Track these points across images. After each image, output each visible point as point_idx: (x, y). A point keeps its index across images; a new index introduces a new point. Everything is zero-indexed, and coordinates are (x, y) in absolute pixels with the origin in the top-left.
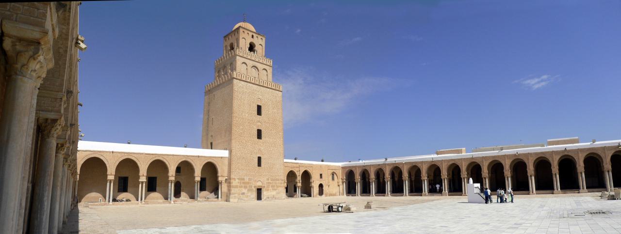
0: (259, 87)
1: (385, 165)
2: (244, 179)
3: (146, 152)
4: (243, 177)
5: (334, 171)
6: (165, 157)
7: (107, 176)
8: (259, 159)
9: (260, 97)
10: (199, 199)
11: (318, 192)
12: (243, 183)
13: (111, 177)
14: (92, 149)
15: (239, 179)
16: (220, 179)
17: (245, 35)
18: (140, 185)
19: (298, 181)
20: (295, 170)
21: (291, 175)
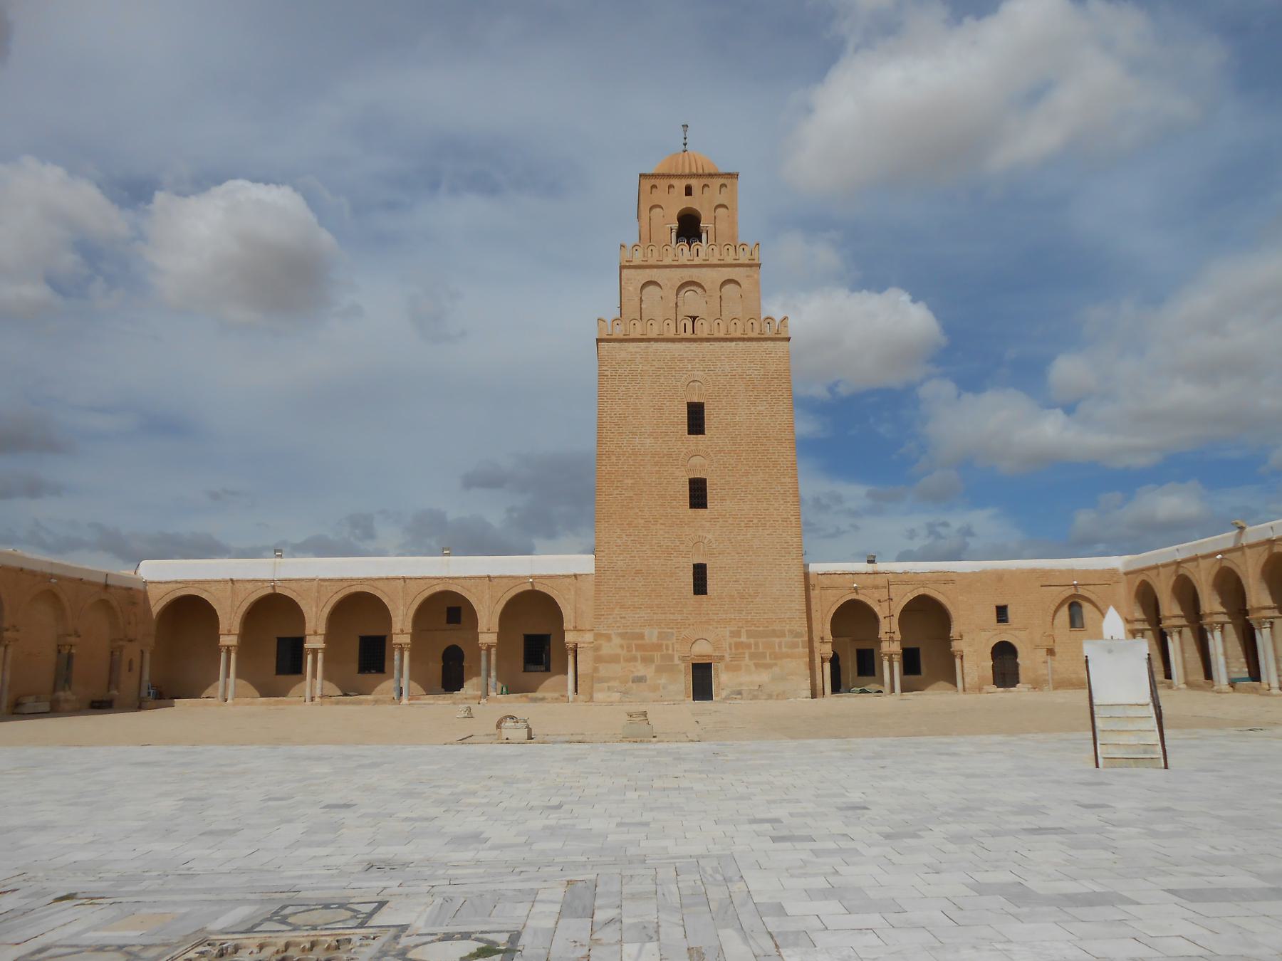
0: (695, 345)
1: (1239, 549)
2: (642, 636)
3: (321, 577)
4: (637, 631)
5: (1081, 591)
6: (380, 584)
7: (217, 637)
8: (700, 574)
9: (699, 375)
10: (493, 694)
11: (989, 673)
12: (639, 647)
13: (229, 639)
14: (180, 578)
15: (623, 636)
16: (569, 637)
17: (660, 196)
18: (309, 658)
19: (882, 635)
20: (869, 599)
21: (854, 617)
